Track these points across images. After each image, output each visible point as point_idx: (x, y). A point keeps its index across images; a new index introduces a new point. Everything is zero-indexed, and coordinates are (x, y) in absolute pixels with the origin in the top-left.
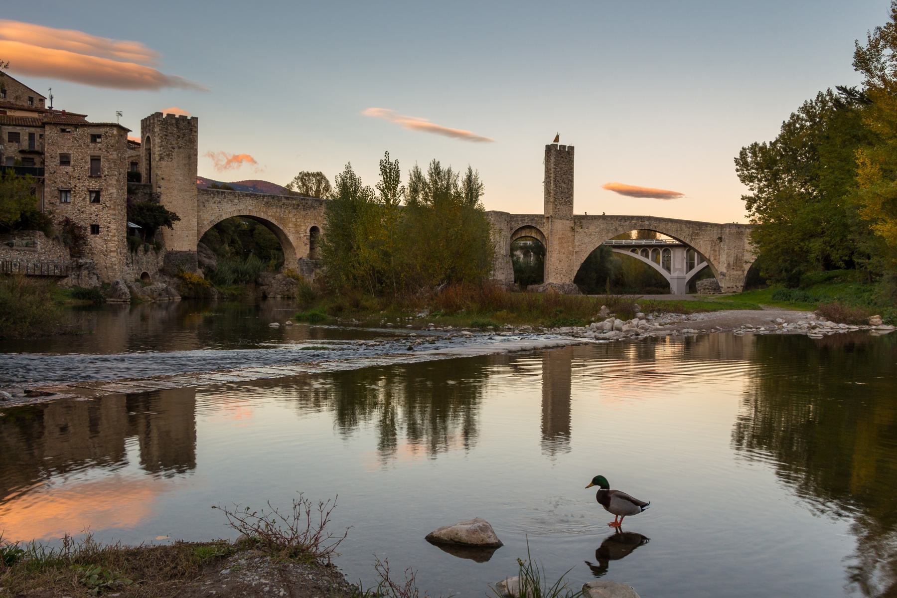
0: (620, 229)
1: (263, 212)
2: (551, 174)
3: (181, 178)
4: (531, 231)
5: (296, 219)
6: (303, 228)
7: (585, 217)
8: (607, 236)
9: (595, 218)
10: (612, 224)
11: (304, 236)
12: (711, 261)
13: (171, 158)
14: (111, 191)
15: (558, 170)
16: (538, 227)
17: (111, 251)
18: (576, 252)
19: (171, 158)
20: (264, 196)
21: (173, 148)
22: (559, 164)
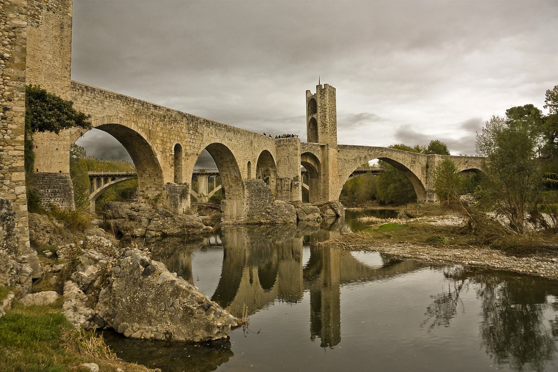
0: (368, 157)
1: (134, 122)
3: (50, 56)
4: (306, 158)
5: (163, 133)
6: (169, 144)
7: (344, 147)
8: (360, 163)
9: (352, 148)
10: (363, 153)
11: (170, 155)
12: (422, 182)
13: (37, 22)
14: (16, 22)
17: (13, 170)
19: (37, 22)
20: (134, 101)
21: (41, 8)
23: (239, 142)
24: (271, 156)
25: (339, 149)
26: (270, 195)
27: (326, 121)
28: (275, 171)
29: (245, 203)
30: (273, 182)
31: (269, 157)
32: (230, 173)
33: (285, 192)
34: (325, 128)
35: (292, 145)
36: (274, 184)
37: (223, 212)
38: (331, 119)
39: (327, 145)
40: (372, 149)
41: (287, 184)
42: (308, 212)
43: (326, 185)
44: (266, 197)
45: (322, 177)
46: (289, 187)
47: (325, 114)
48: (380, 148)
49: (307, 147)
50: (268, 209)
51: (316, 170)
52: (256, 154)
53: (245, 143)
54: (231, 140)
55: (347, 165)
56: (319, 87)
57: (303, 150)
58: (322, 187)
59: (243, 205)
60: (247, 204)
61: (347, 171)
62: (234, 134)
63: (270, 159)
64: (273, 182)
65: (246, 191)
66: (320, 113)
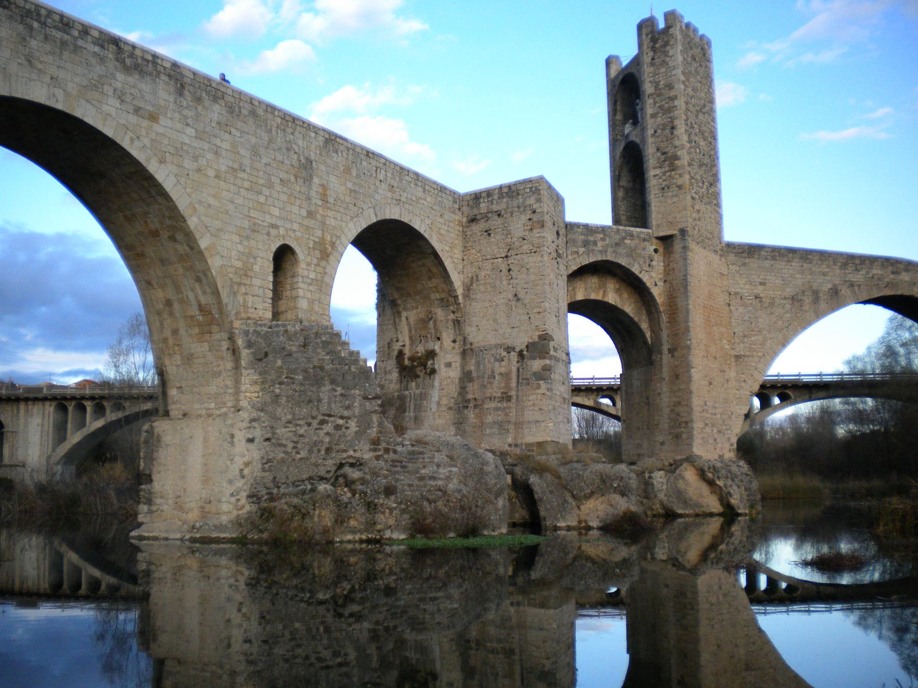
0: (845, 291)
7: (751, 251)
10: (824, 274)
16: (635, 269)
18: (737, 357)
23: (218, 142)
25: (731, 257)
26: (366, 398)
27: (677, 143)
28: (457, 323)
29: (240, 436)
30: (449, 365)
31: (429, 262)
32: (178, 289)
33: (492, 405)
34: (673, 168)
35: (522, 208)
36: (454, 373)
37: (149, 479)
39: (683, 232)
40: (857, 262)
41: (503, 370)
42: (581, 489)
43: (683, 386)
44: (348, 408)
45: (666, 358)
46: (508, 386)
47: (672, 120)
48: (888, 262)
49: (603, 239)
50: (352, 465)
51: (643, 335)
52: (331, 222)
53: (255, 153)
54: (153, 118)
56: (646, 28)
57: (588, 253)
58: (665, 400)
59: (232, 444)
60: (251, 441)
61: (763, 344)
62: (181, 94)
63: (434, 270)
64: (449, 365)
65: (249, 381)
66: (654, 116)
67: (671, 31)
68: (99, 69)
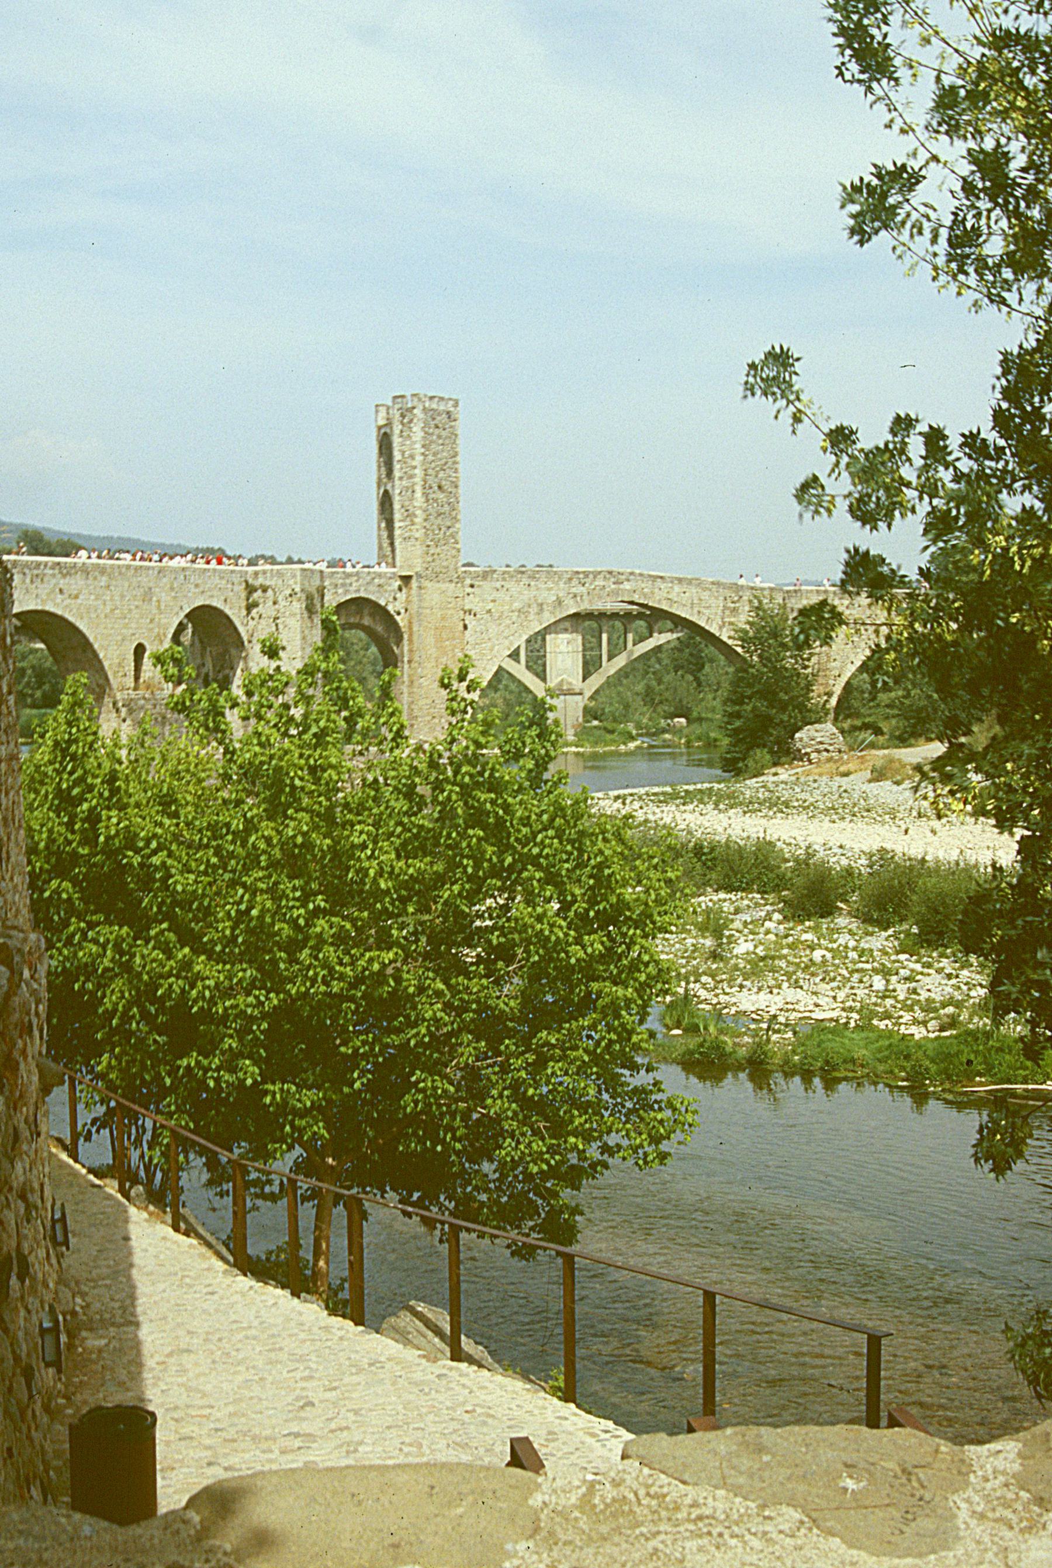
0: (569, 601)
2: (415, 467)
15: (431, 458)
22: (432, 442)
24: (227, 617)
38: (431, 496)
45: (406, 666)
47: (414, 484)
53: (122, 596)
55: (493, 630)
61: (491, 650)
66: (401, 478)
67: (415, 411)
68: (54, 581)
